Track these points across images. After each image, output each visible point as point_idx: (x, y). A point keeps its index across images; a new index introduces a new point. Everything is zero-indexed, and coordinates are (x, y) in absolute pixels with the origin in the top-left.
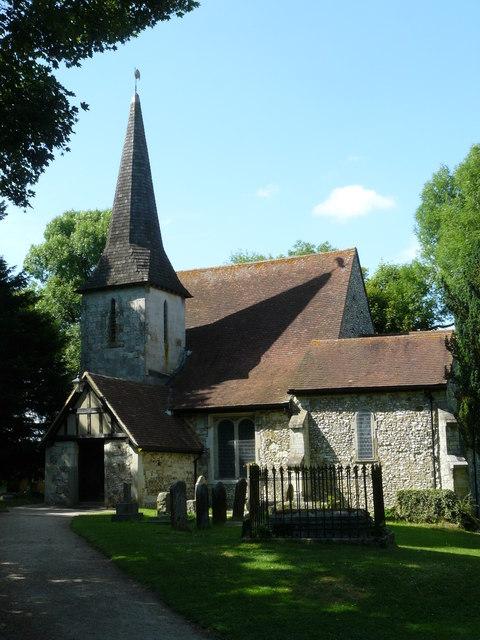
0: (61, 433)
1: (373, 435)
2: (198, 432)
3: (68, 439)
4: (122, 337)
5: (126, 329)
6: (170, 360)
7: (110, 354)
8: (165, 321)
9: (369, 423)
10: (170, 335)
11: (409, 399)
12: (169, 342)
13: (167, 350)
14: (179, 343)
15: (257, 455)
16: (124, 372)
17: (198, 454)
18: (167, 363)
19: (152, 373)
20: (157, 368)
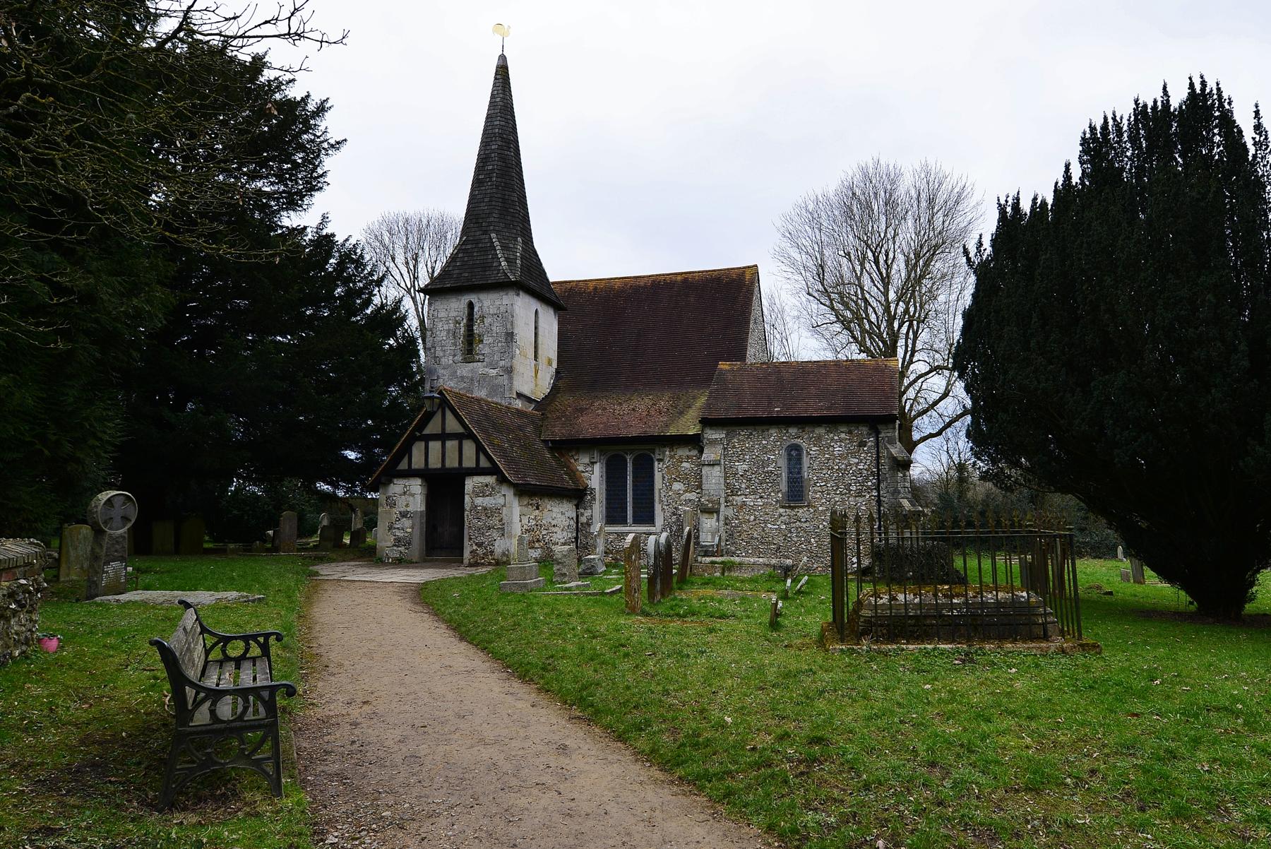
2: (581, 468)
4: (479, 348)
6: (540, 382)
7: (465, 370)
8: (536, 335)
10: (540, 352)
11: (850, 432)
12: (539, 360)
15: (657, 498)
17: (578, 495)
19: (520, 396)
20: (526, 390)
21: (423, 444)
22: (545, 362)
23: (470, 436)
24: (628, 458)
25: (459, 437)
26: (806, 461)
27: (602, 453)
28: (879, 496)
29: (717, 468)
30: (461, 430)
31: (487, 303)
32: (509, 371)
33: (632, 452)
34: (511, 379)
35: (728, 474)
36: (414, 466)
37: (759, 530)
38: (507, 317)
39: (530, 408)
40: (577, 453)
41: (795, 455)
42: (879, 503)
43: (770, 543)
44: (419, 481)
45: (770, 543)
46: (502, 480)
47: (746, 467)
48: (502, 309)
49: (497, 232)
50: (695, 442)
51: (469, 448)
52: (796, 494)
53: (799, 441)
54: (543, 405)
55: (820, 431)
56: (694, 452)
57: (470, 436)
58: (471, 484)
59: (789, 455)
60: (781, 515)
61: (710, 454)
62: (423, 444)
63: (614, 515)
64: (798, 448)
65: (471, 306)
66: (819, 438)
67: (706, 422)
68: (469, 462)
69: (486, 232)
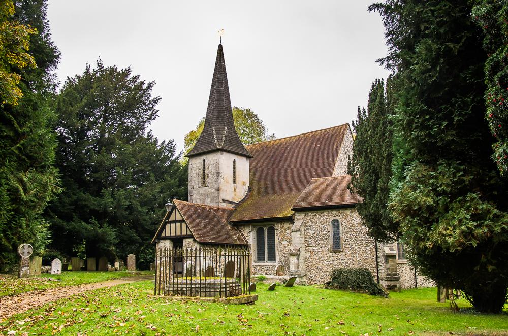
0: (163, 235)
1: (341, 235)
3: (165, 238)
4: (208, 180)
5: (210, 176)
7: (202, 191)
8: (234, 172)
9: (339, 227)
10: (237, 179)
13: (235, 189)
14: (244, 184)
16: (209, 201)
18: (235, 195)
19: (224, 201)
21: (169, 225)
22: (241, 184)
23: (184, 221)
24: (265, 229)
25: (182, 221)
26: (341, 227)
27: (254, 227)
28: (376, 246)
29: (299, 233)
30: (181, 219)
31: (210, 159)
32: (218, 190)
33: (265, 226)
34: (219, 193)
35: (307, 236)
36: (167, 235)
37: (321, 264)
38: (217, 165)
39: (231, 207)
40: (244, 227)
41: (336, 224)
42: (377, 249)
43: (326, 271)
44: (168, 241)
45: (326, 271)
46: (195, 241)
47: (314, 232)
48: (215, 162)
49: (215, 126)
50: (290, 220)
51: (184, 225)
52: (337, 246)
53: (337, 218)
54: (238, 205)
55: (347, 212)
56: (291, 225)
57: (184, 221)
58: (186, 242)
59: (334, 225)
60: (330, 257)
61: (297, 224)
62: (169, 225)
63: (260, 258)
64: (337, 221)
65: (204, 161)
66: (347, 216)
67: (297, 210)
68: (184, 233)
69: (211, 127)
